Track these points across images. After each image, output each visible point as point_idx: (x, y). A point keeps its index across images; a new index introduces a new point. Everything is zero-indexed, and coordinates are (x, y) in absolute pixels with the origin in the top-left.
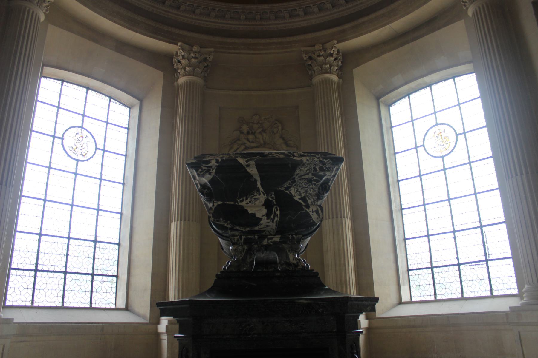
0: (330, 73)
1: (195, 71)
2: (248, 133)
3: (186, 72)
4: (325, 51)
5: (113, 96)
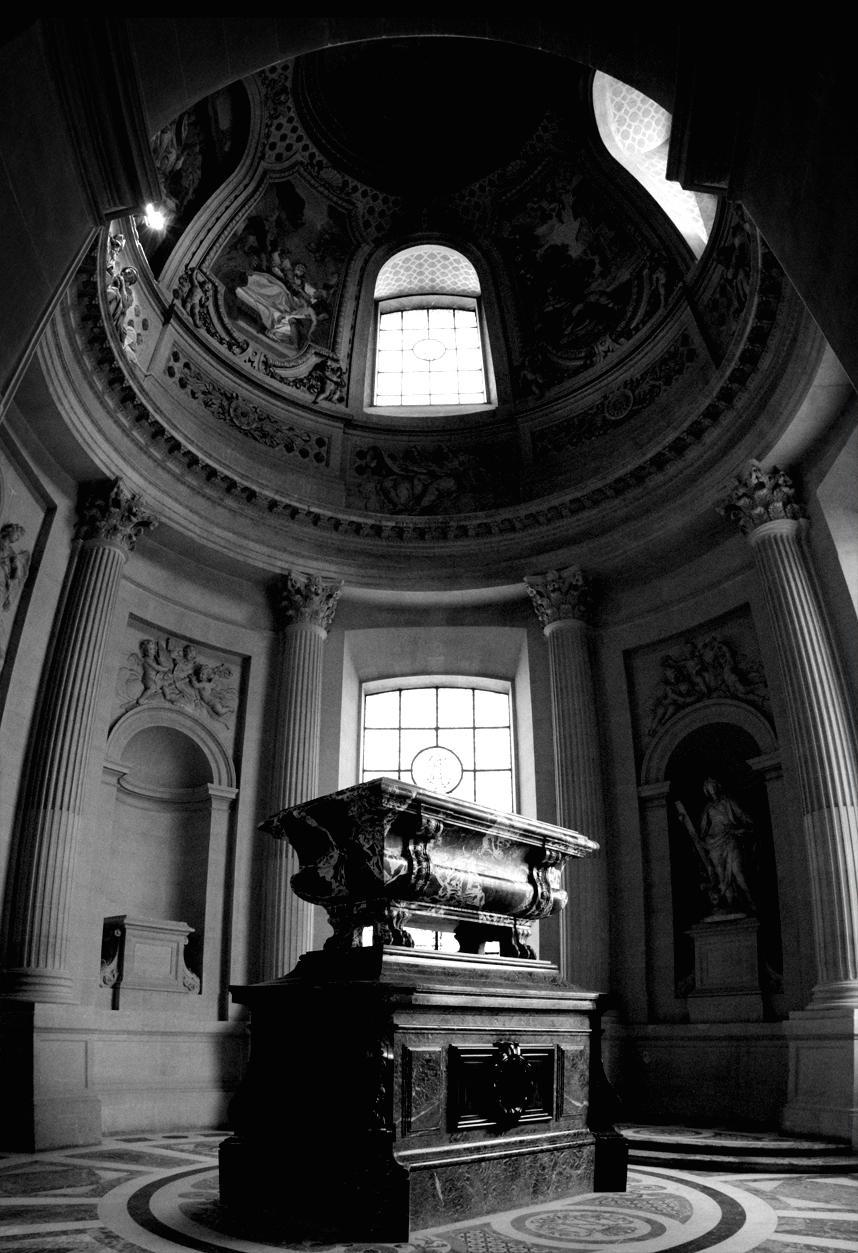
2: (678, 681)
5: (474, 686)
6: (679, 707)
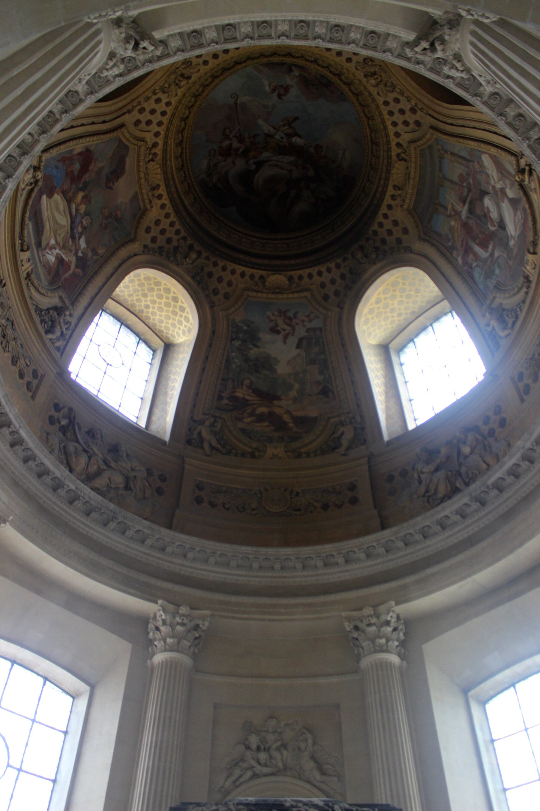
0: (387, 651)
1: (180, 644)
2: (258, 749)
3: (167, 646)
4: (378, 617)
5: (50, 676)
6: (255, 776)
